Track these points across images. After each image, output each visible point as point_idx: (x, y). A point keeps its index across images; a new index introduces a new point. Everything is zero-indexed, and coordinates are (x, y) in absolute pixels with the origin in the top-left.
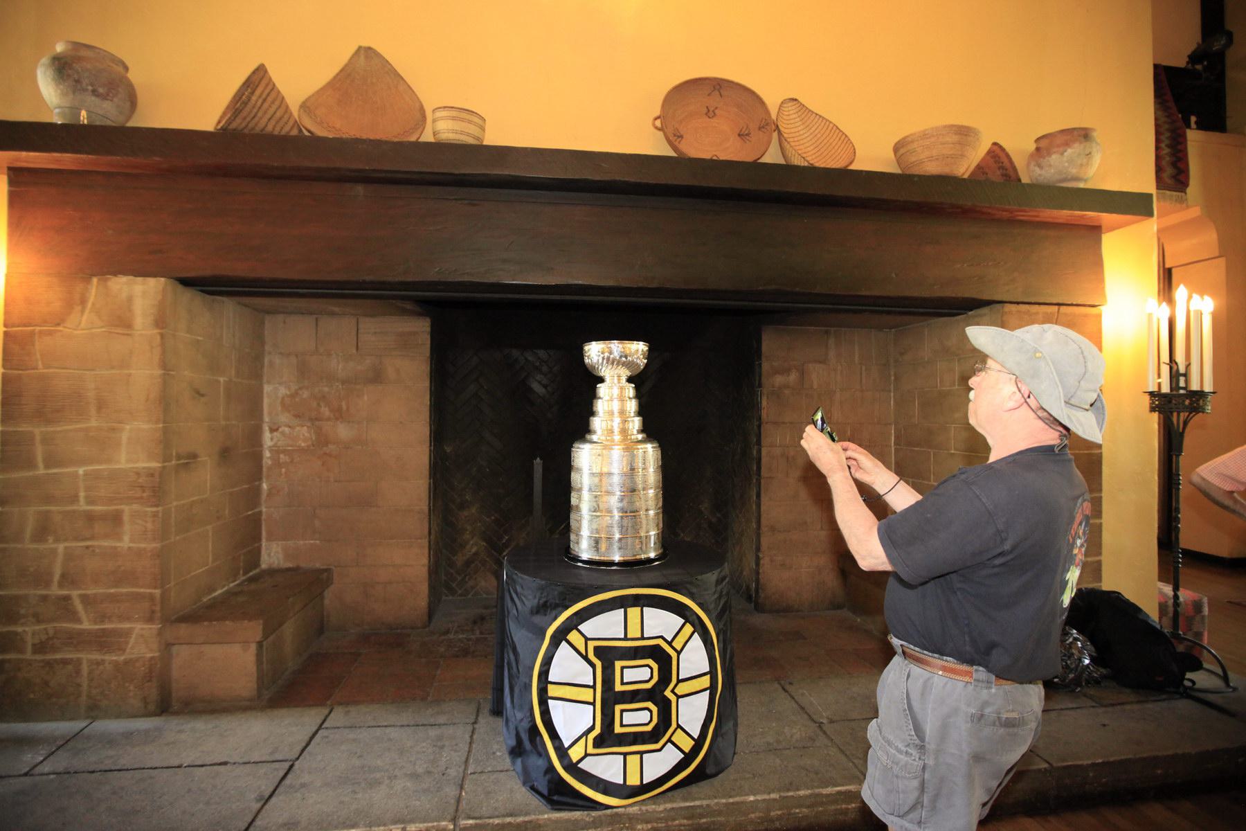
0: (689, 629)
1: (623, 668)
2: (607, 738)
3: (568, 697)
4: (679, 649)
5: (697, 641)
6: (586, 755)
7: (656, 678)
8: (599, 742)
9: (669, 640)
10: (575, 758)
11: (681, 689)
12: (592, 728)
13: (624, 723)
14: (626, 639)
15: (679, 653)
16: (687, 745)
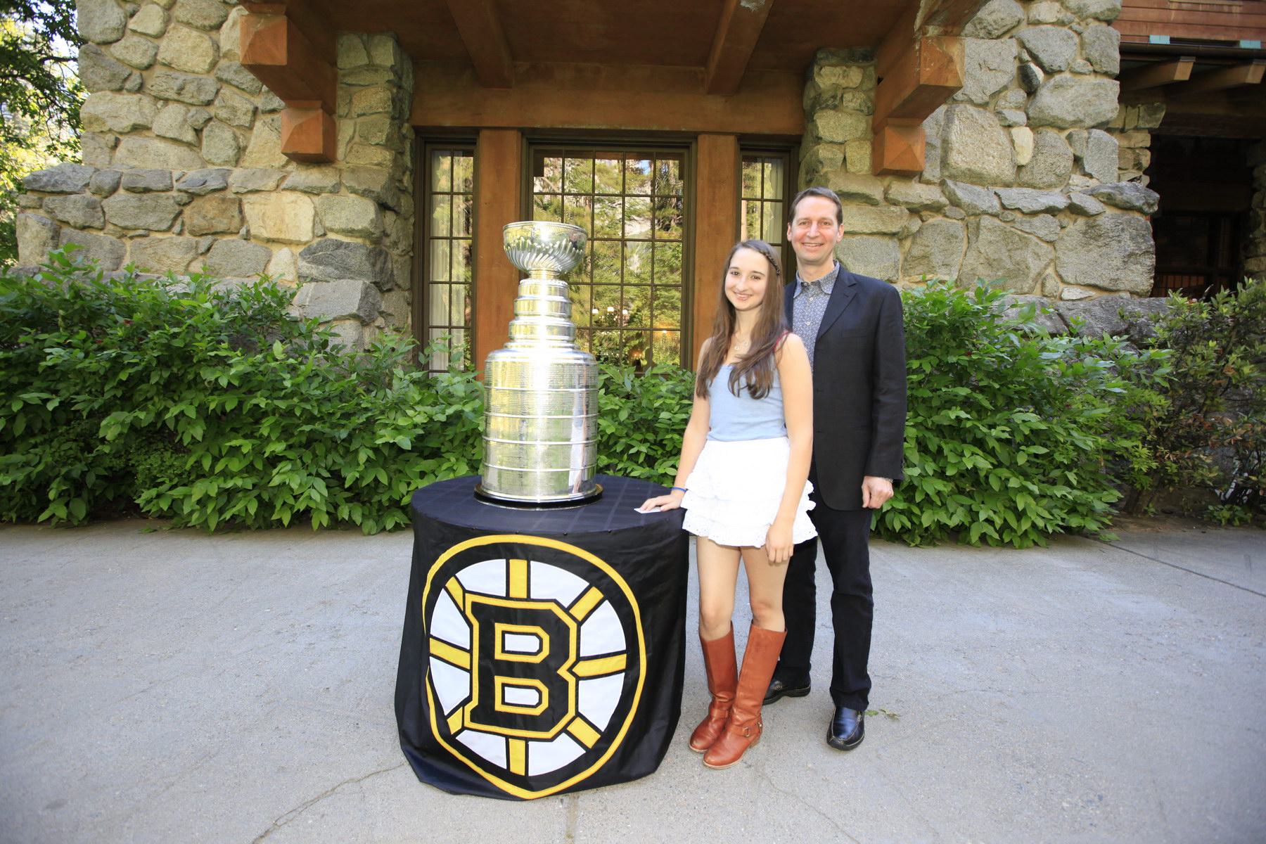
0: (595, 595)
1: (504, 633)
2: (485, 714)
3: (446, 658)
4: (580, 618)
5: (607, 609)
6: (464, 728)
7: (546, 652)
8: (475, 716)
9: (566, 605)
10: (453, 730)
11: (581, 669)
12: (469, 699)
13: (506, 701)
14: (508, 597)
15: (580, 624)
16: (591, 738)
